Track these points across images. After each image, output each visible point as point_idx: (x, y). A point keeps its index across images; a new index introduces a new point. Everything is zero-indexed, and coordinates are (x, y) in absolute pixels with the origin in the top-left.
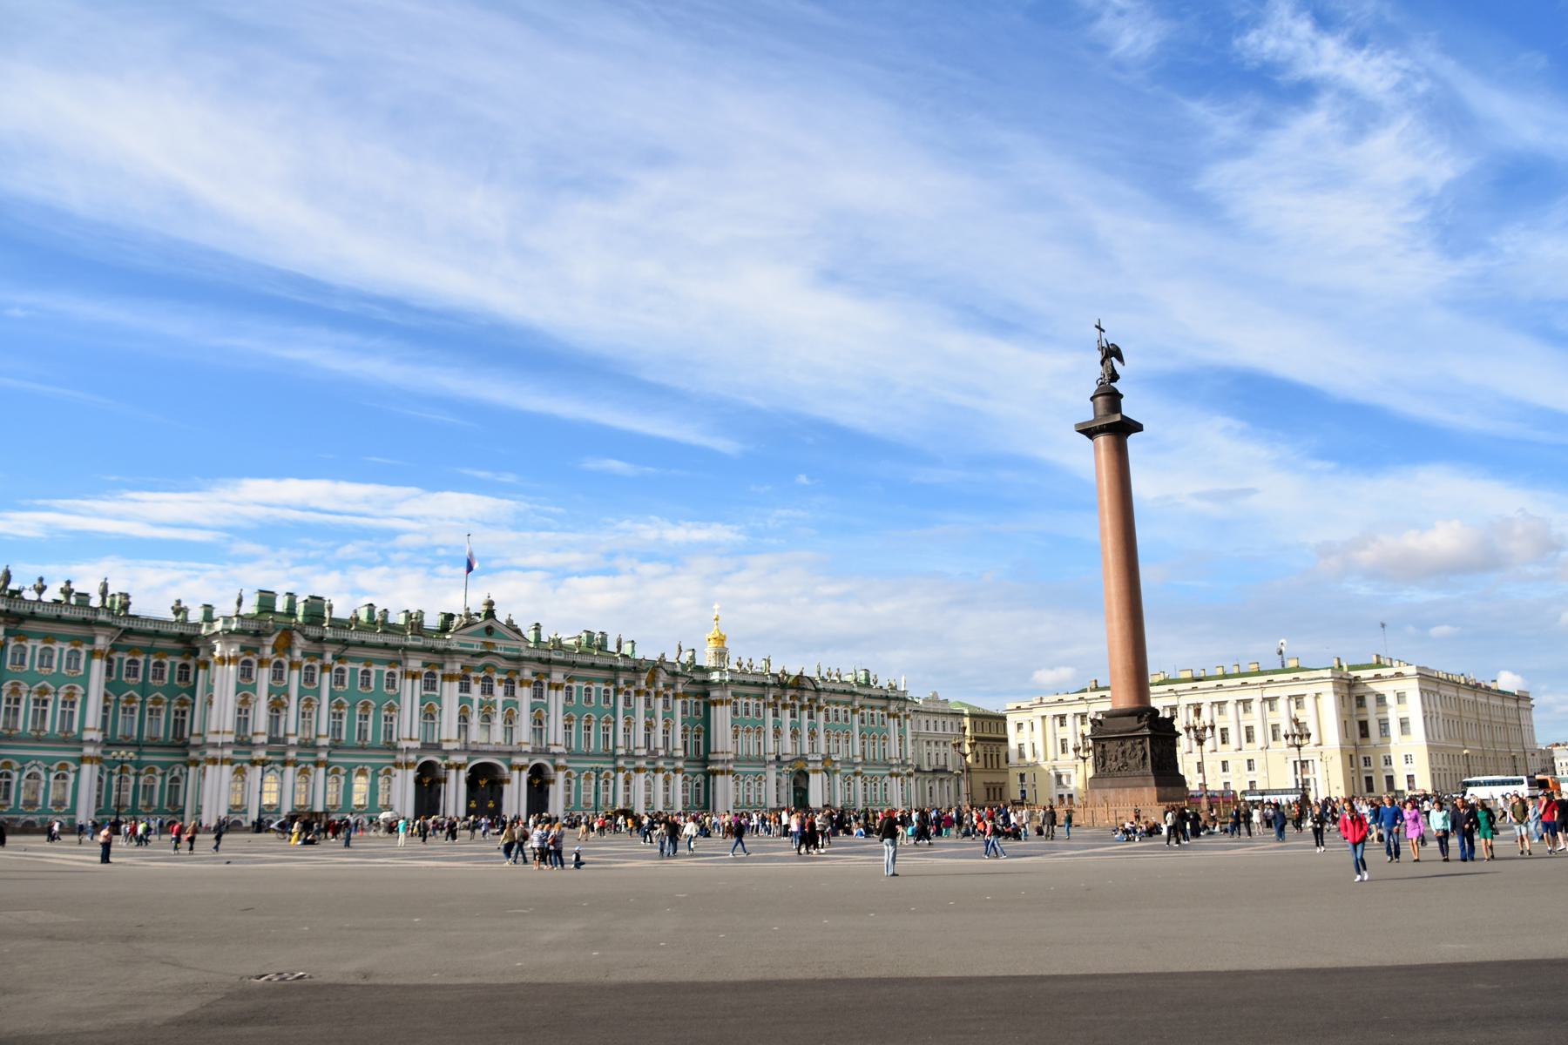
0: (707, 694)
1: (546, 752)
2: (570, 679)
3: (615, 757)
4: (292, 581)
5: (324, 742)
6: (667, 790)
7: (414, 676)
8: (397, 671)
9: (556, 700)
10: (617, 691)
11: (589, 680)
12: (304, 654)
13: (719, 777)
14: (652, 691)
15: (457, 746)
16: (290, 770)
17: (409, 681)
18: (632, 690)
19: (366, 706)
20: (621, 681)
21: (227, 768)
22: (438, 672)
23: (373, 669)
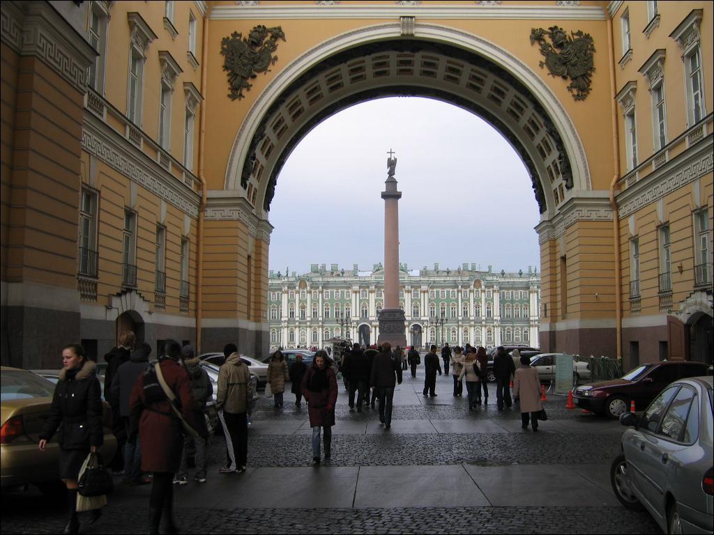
0: (529, 288)
1: (419, 320)
2: (432, 287)
3: (458, 321)
4: (327, 260)
5: (320, 319)
6: (491, 335)
7: (356, 292)
8: (350, 290)
9: (424, 299)
10: (458, 291)
11: (443, 287)
12: (311, 288)
13: (531, 328)
14: (480, 290)
15: (374, 319)
16: (308, 329)
17: (354, 295)
18: (468, 290)
19: (337, 304)
20: (460, 287)
21: (286, 329)
22: (367, 290)
23: (339, 291)
